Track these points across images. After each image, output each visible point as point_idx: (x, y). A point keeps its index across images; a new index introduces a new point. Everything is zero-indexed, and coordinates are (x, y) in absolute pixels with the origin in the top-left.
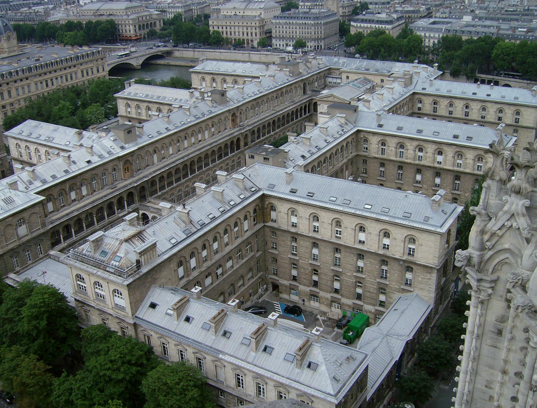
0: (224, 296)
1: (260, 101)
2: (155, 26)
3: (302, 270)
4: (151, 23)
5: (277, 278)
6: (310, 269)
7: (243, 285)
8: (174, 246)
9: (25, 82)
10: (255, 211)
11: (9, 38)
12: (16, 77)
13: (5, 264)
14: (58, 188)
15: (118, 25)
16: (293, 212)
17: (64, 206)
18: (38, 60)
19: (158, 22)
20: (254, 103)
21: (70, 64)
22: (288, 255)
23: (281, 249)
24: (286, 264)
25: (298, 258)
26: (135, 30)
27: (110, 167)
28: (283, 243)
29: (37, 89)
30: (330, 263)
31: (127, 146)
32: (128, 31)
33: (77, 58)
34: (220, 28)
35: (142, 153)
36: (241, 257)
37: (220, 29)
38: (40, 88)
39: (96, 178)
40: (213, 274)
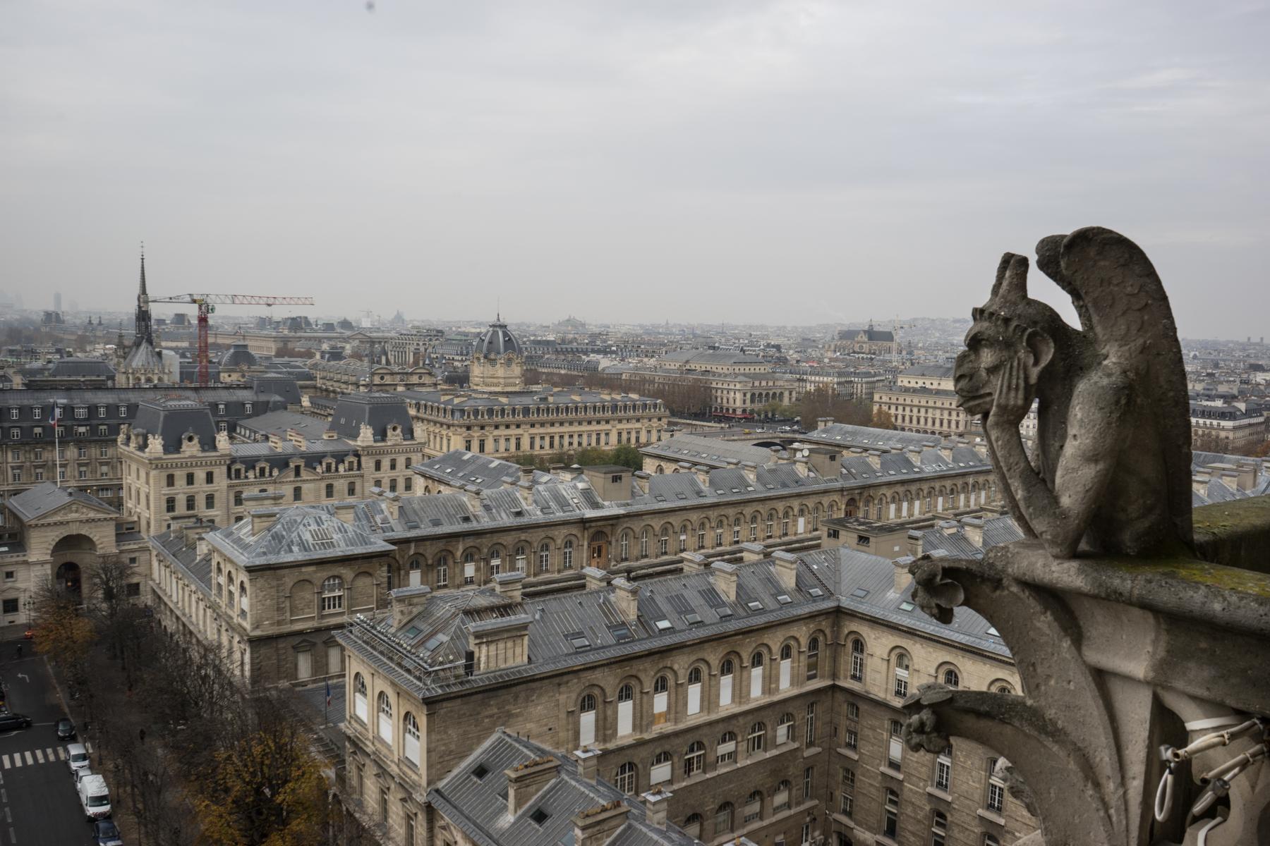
0: (702, 825)
1: (913, 488)
2: (781, 400)
3: (909, 811)
4: (774, 394)
5: (852, 824)
6: (928, 808)
7: (760, 815)
8: (579, 651)
9: (513, 431)
10: (814, 644)
11: (509, 362)
12: (499, 419)
13: (279, 660)
14: (441, 545)
15: (717, 389)
16: (901, 656)
17: (445, 586)
18: (546, 399)
19: (786, 394)
20: (900, 489)
21: (599, 415)
22: (879, 765)
23: (865, 749)
24: (872, 790)
25: (901, 777)
26: (744, 402)
27: (560, 535)
28: (870, 733)
29: (532, 446)
30: (977, 797)
31: (606, 503)
32: (731, 401)
33: (615, 408)
34: (893, 408)
35: (637, 526)
36: (758, 743)
37: (893, 411)
38: (537, 446)
39: (527, 551)
40: (676, 759)
